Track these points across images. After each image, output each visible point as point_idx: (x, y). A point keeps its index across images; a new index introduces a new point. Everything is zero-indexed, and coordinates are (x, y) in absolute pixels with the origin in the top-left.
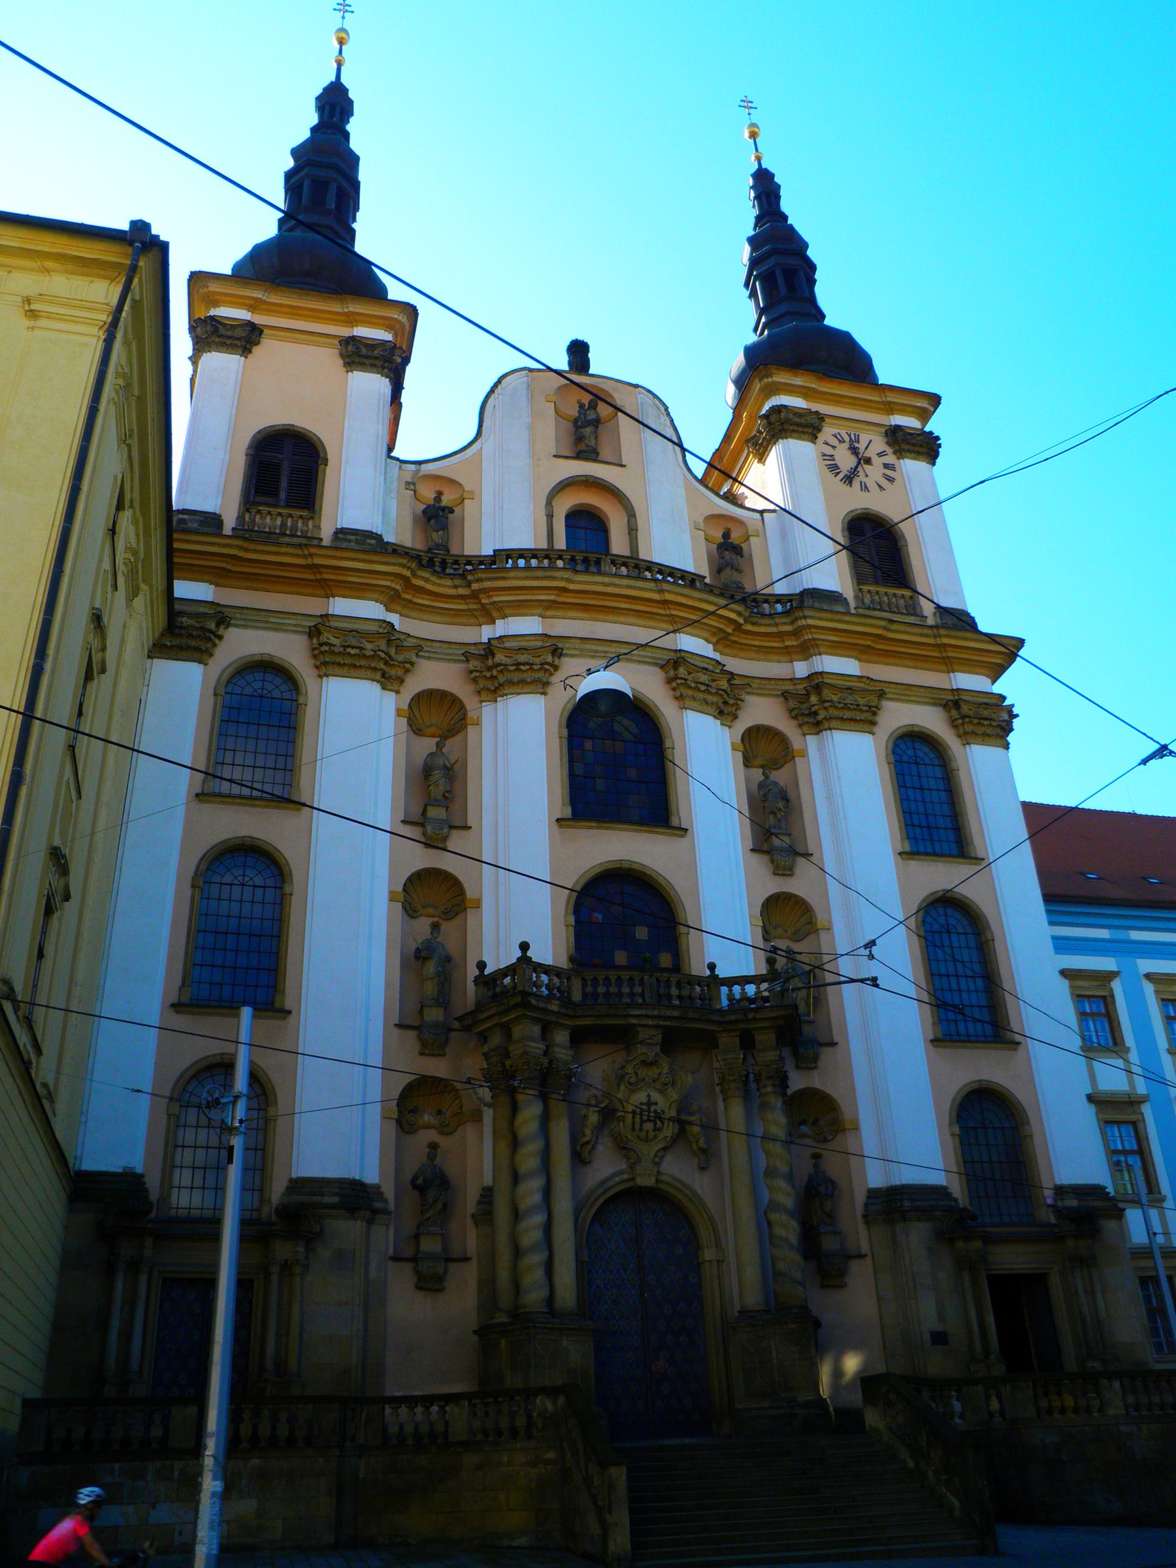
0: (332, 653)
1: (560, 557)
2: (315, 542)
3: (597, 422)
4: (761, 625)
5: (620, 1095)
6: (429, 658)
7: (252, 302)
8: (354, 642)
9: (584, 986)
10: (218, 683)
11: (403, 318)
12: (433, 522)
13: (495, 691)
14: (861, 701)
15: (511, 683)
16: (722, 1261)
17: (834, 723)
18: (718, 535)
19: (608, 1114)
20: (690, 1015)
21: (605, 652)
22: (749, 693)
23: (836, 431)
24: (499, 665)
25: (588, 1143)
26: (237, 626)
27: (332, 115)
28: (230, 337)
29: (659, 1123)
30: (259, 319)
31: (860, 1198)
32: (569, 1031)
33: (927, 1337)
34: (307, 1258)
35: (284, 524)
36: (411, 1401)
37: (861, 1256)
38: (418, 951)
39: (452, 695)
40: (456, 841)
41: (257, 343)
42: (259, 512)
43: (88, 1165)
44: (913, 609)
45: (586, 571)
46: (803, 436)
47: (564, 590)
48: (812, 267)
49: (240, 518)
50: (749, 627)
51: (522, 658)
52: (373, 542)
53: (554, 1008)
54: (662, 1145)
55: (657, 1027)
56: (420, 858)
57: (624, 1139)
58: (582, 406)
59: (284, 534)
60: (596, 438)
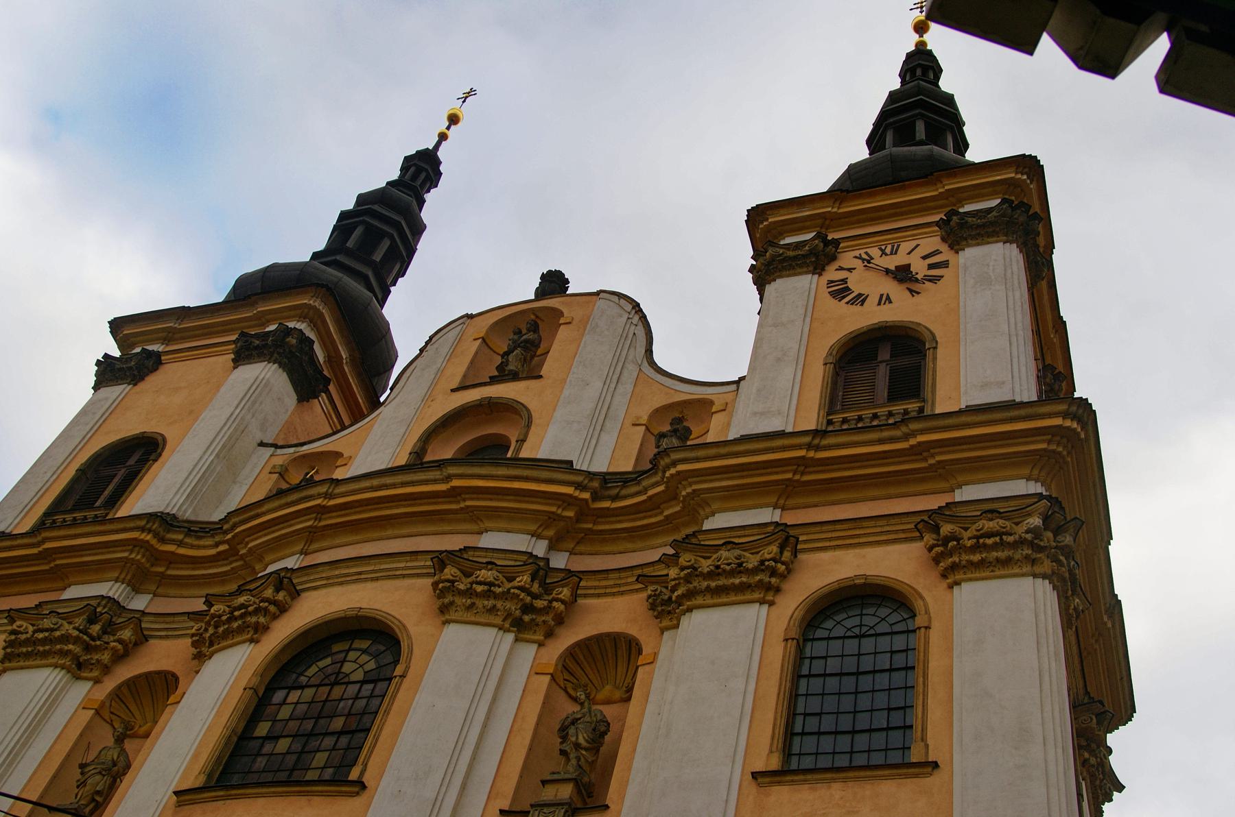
4: (625, 497)
17: (699, 600)
21: (360, 573)
27: (415, 177)
47: (321, 511)
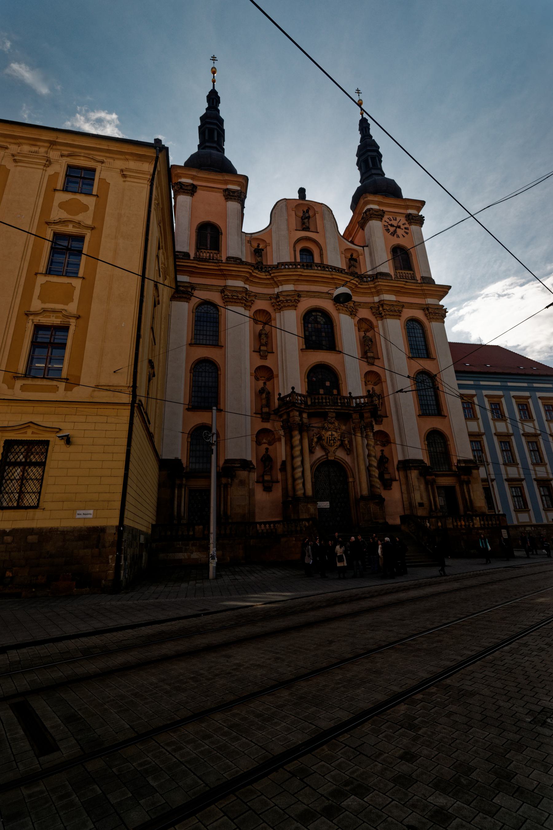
0: (229, 298)
1: (299, 265)
2: (220, 261)
3: (309, 217)
5: (323, 433)
6: (259, 299)
7: (192, 176)
8: (235, 294)
9: (311, 400)
10: (193, 309)
11: (243, 181)
12: (257, 254)
13: (280, 309)
14: (396, 309)
15: (285, 306)
17: (387, 316)
18: (349, 256)
19: (320, 439)
20: (344, 408)
22: (359, 308)
23: (388, 217)
24: (281, 300)
25: (314, 447)
26: (197, 290)
28: (186, 190)
30: (196, 183)
31: (396, 463)
33: (417, 504)
34: (231, 482)
35: (210, 256)
36: (265, 523)
37: (396, 480)
38: (260, 391)
39: (266, 311)
40: (270, 356)
41: (196, 192)
42: (201, 252)
43: (164, 457)
44: (413, 278)
45: (307, 269)
46: (378, 219)
47: (301, 275)
48: (380, 156)
49: (196, 254)
50: (360, 286)
51: (288, 298)
52: (239, 261)
53: (303, 407)
54: (336, 447)
55: (334, 412)
56: (260, 362)
58: (304, 212)
59: (210, 259)
60: (309, 223)
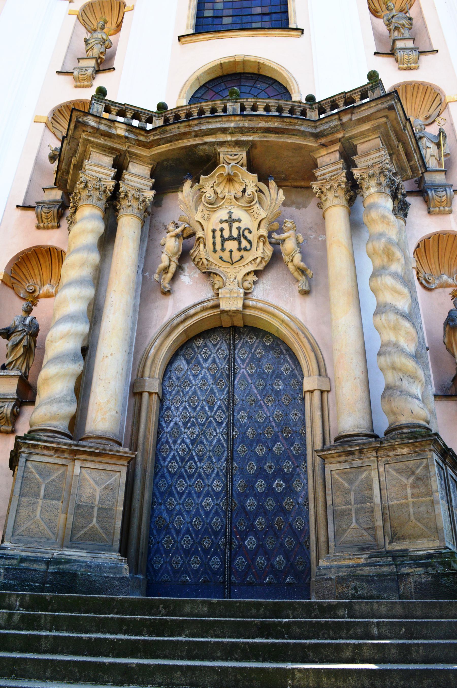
5: (198, 217)
16: (328, 392)
25: (166, 270)
29: (244, 243)
32: (151, 167)
54: (251, 268)
55: (238, 144)
57: (205, 262)
